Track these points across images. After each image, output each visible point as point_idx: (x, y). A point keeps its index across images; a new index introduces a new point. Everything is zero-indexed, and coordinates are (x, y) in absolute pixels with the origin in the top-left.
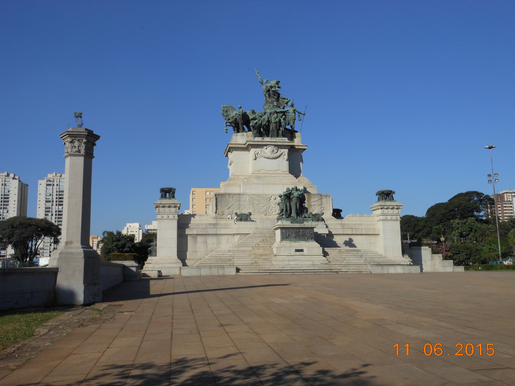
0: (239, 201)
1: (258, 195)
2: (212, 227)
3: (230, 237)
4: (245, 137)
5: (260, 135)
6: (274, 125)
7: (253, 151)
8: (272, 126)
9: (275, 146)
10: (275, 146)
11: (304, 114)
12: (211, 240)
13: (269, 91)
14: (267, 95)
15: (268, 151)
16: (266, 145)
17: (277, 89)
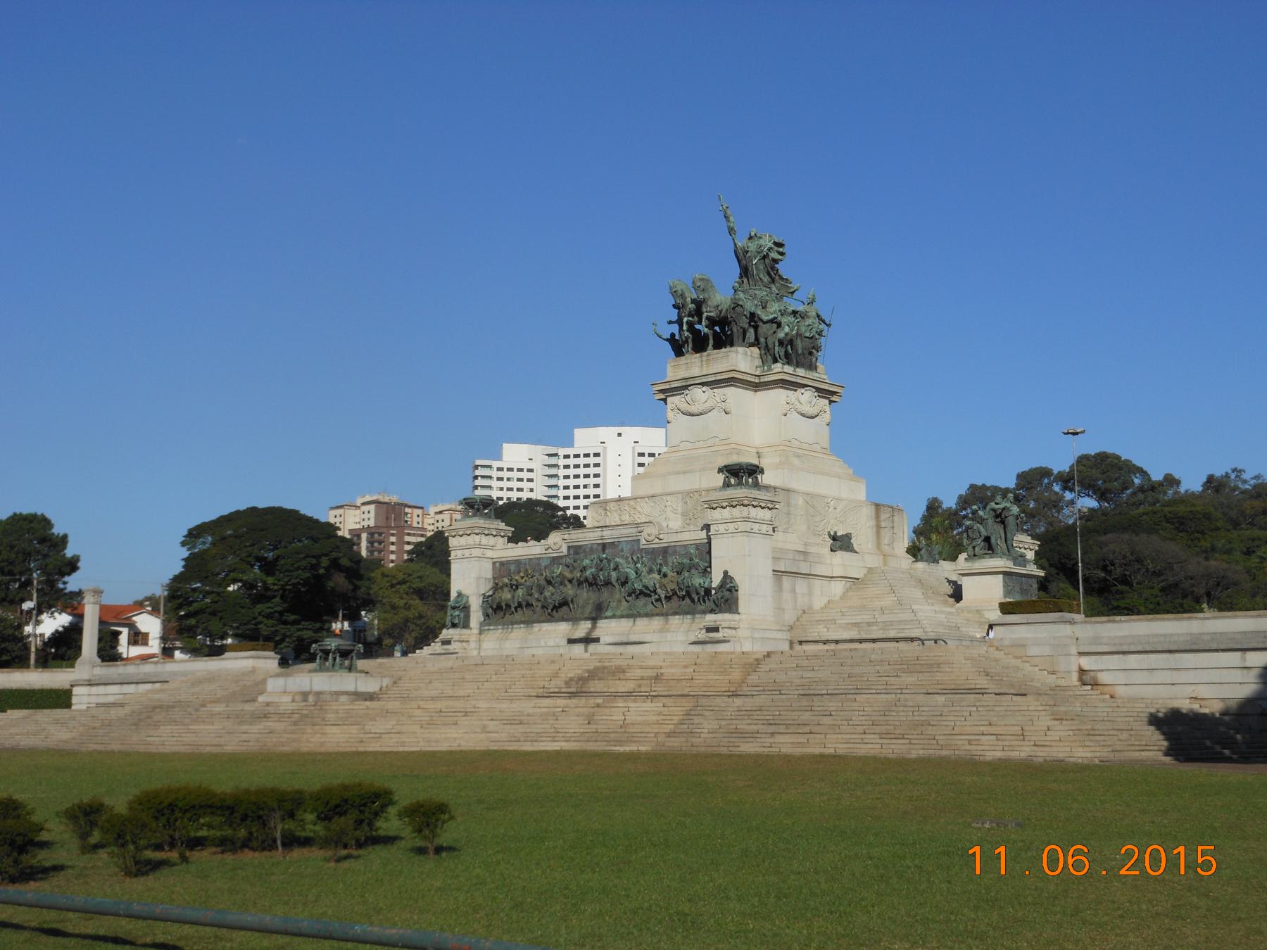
1: (813, 496)
2: (801, 558)
3: (825, 582)
5: (788, 360)
7: (780, 395)
8: (799, 343)
9: (818, 390)
10: (818, 390)
11: (829, 325)
12: (801, 585)
13: (764, 257)
14: (761, 267)
15: (806, 398)
16: (804, 386)
17: (777, 256)
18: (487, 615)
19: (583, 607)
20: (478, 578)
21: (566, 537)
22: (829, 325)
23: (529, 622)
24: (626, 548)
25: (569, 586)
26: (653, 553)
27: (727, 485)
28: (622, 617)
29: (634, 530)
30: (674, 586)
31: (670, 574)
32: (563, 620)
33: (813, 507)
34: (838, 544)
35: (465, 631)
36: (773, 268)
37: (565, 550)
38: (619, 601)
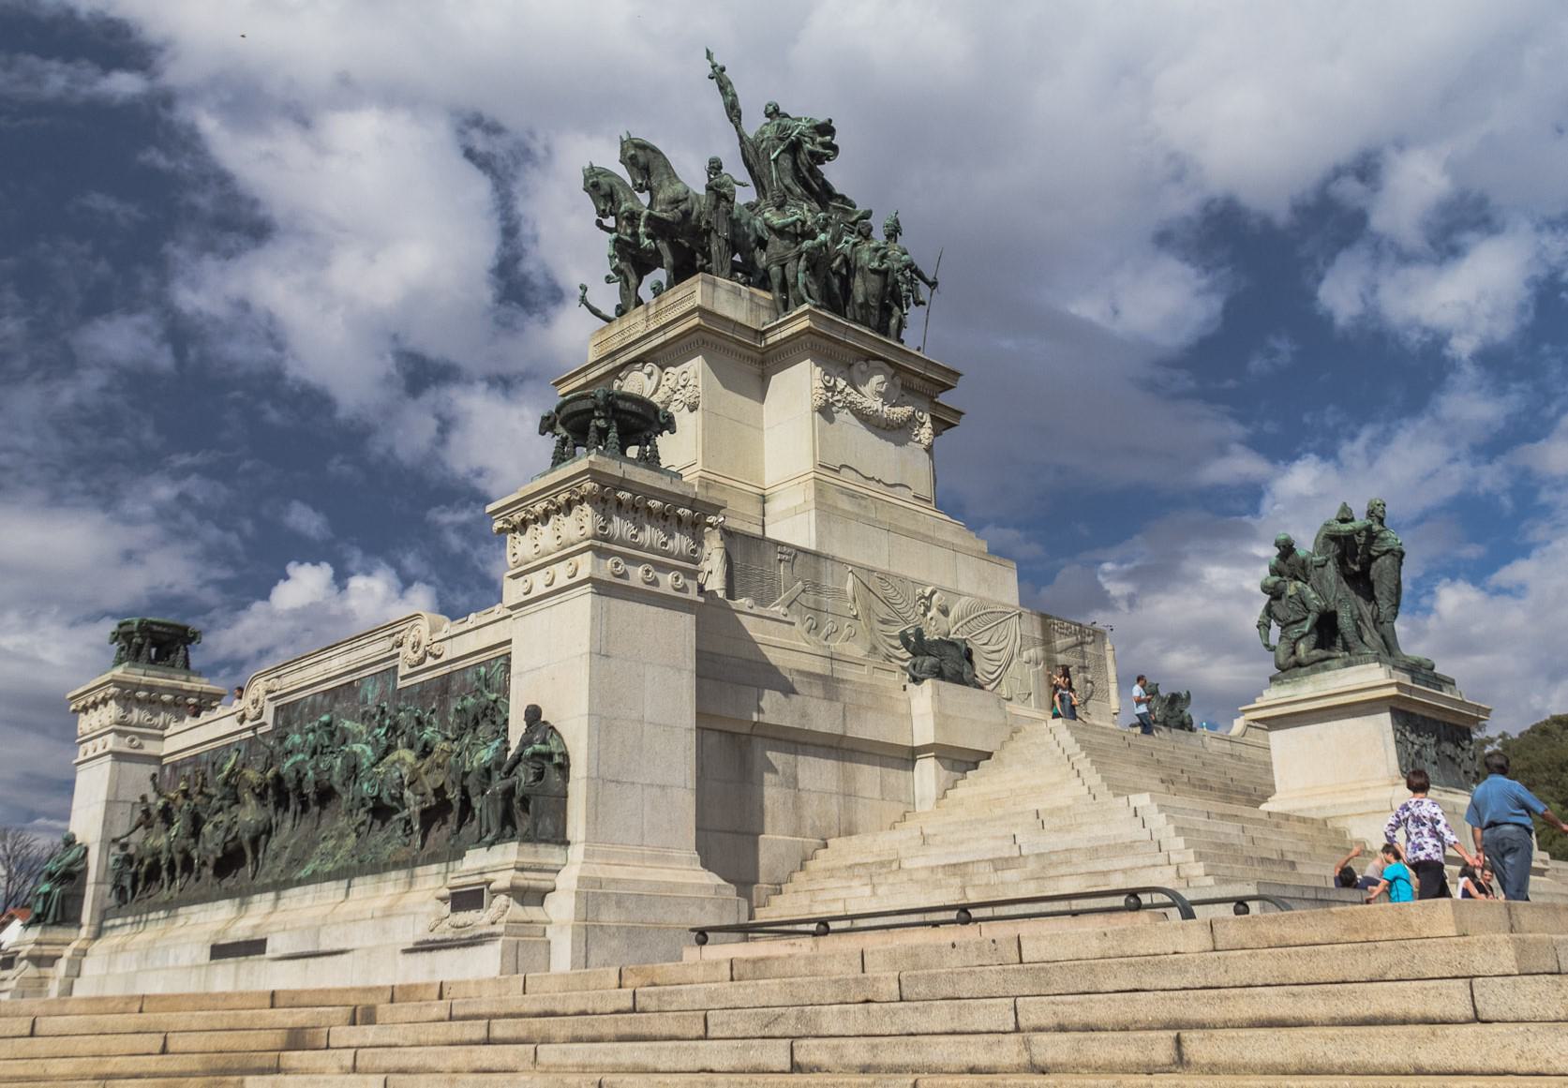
0: (817, 587)
4: (746, 304)
6: (875, 283)
8: (859, 288)
11: (933, 285)
13: (794, 148)
18: (120, 891)
19: (276, 856)
20: (111, 803)
21: (277, 684)
22: (933, 285)
23: (171, 906)
24: (372, 694)
25: (251, 803)
26: (422, 692)
27: (559, 459)
28: (330, 877)
29: (388, 643)
30: (437, 779)
31: (441, 745)
32: (229, 894)
33: (887, 602)
34: (928, 661)
35: (59, 934)
36: (812, 170)
37: (268, 717)
38: (342, 836)
